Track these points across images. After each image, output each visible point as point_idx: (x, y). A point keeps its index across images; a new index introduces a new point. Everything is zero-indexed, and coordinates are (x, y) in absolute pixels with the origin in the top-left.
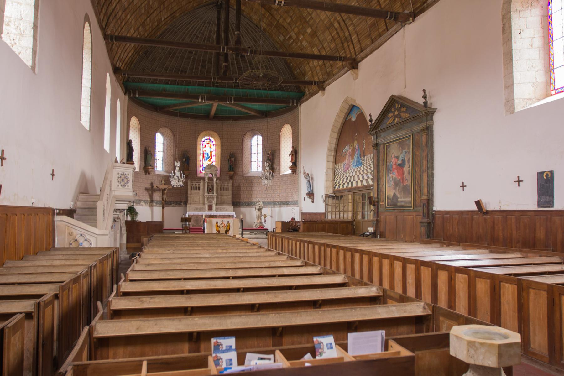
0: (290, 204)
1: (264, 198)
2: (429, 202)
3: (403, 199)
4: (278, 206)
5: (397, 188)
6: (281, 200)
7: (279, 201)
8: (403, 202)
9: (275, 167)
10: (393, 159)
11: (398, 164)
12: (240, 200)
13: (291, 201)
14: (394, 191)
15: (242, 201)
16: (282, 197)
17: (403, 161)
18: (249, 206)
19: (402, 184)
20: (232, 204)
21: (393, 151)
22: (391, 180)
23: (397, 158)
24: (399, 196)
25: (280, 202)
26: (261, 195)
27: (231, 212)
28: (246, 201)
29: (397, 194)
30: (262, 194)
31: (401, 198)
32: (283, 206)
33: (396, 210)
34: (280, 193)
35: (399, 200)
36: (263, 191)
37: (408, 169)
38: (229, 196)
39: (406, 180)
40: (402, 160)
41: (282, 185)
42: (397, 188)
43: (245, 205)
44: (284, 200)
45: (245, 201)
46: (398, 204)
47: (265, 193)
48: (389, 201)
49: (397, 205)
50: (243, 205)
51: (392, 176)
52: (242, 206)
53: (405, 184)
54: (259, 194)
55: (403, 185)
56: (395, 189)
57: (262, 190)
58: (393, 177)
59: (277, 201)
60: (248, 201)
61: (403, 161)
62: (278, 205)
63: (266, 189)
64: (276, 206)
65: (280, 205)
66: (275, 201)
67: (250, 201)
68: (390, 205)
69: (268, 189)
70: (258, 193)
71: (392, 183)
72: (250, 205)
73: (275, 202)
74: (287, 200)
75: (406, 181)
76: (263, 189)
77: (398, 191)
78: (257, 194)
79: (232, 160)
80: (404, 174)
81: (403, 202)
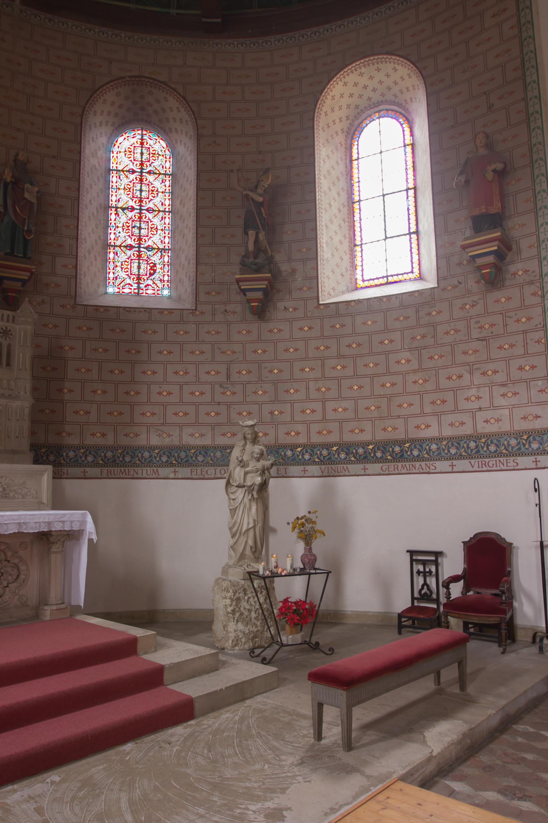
0: (419, 458)
1: (213, 426)
4: (314, 469)
6: (334, 438)
7: (316, 439)
9: (284, 267)
12: (59, 434)
13: (439, 440)
15: (74, 441)
16: (341, 422)
18: (116, 470)
20: (30, 456)
25: (328, 446)
26: (191, 410)
27: (40, 506)
28: (98, 441)
30: (197, 405)
32: (358, 468)
34: (324, 401)
36: (207, 388)
38: (16, 404)
41: (340, 356)
43: (94, 464)
44: (366, 437)
45: (89, 441)
47: (219, 398)
50: (76, 463)
52: (78, 471)
54: (181, 402)
57: (198, 381)
59: (302, 440)
60: (110, 440)
62: (314, 463)
63: (222, 378)
64: (294, 469)
65: (328, 461)
66: (283, 439)
67: (124, 441)
69: (235, 377)
70: (174, 398)
72: (124, 465)
73: (285, 447)
74: (381, 436)
76: (204, 377)
78: (165, 405)
79: (26, 195)
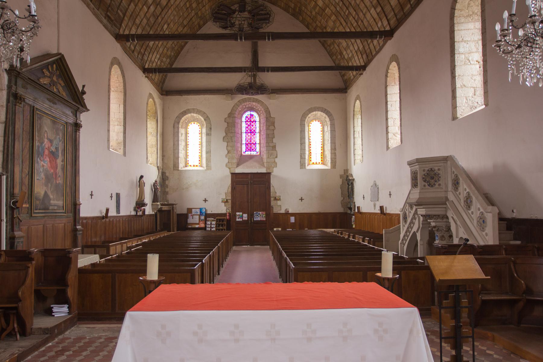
2: (75, 206)
3: (56, 202)
5: (50, 185)
8: (56, 206)
10: (46, 140)
11: (51, 150)
14: (45, 188)
17: (57, 149)
19: (55, 181)
21: (46, 129)
22: (41, 170)
23: (51, 141)
24: (51, 197)
29: (49, 193)
31: (54, 200)
33: (46, 217)
35: (52, 202)
37: (61, 163)
39: (59, 176)
40: (56, 148)
42: (50, 185)
46: (51, 208)
48: (38, 202)
49: (48, 209)
51: (43, 166)
53: (58, 182)
55: (56, 182)
56: (46, 185)
58: (45, 167)
61: (57, 149)
68: (40, 210)
71: (42, 175)
75: (60, 178)
77: (50, 189)
80: (57, 169)
81: (56, 206)
